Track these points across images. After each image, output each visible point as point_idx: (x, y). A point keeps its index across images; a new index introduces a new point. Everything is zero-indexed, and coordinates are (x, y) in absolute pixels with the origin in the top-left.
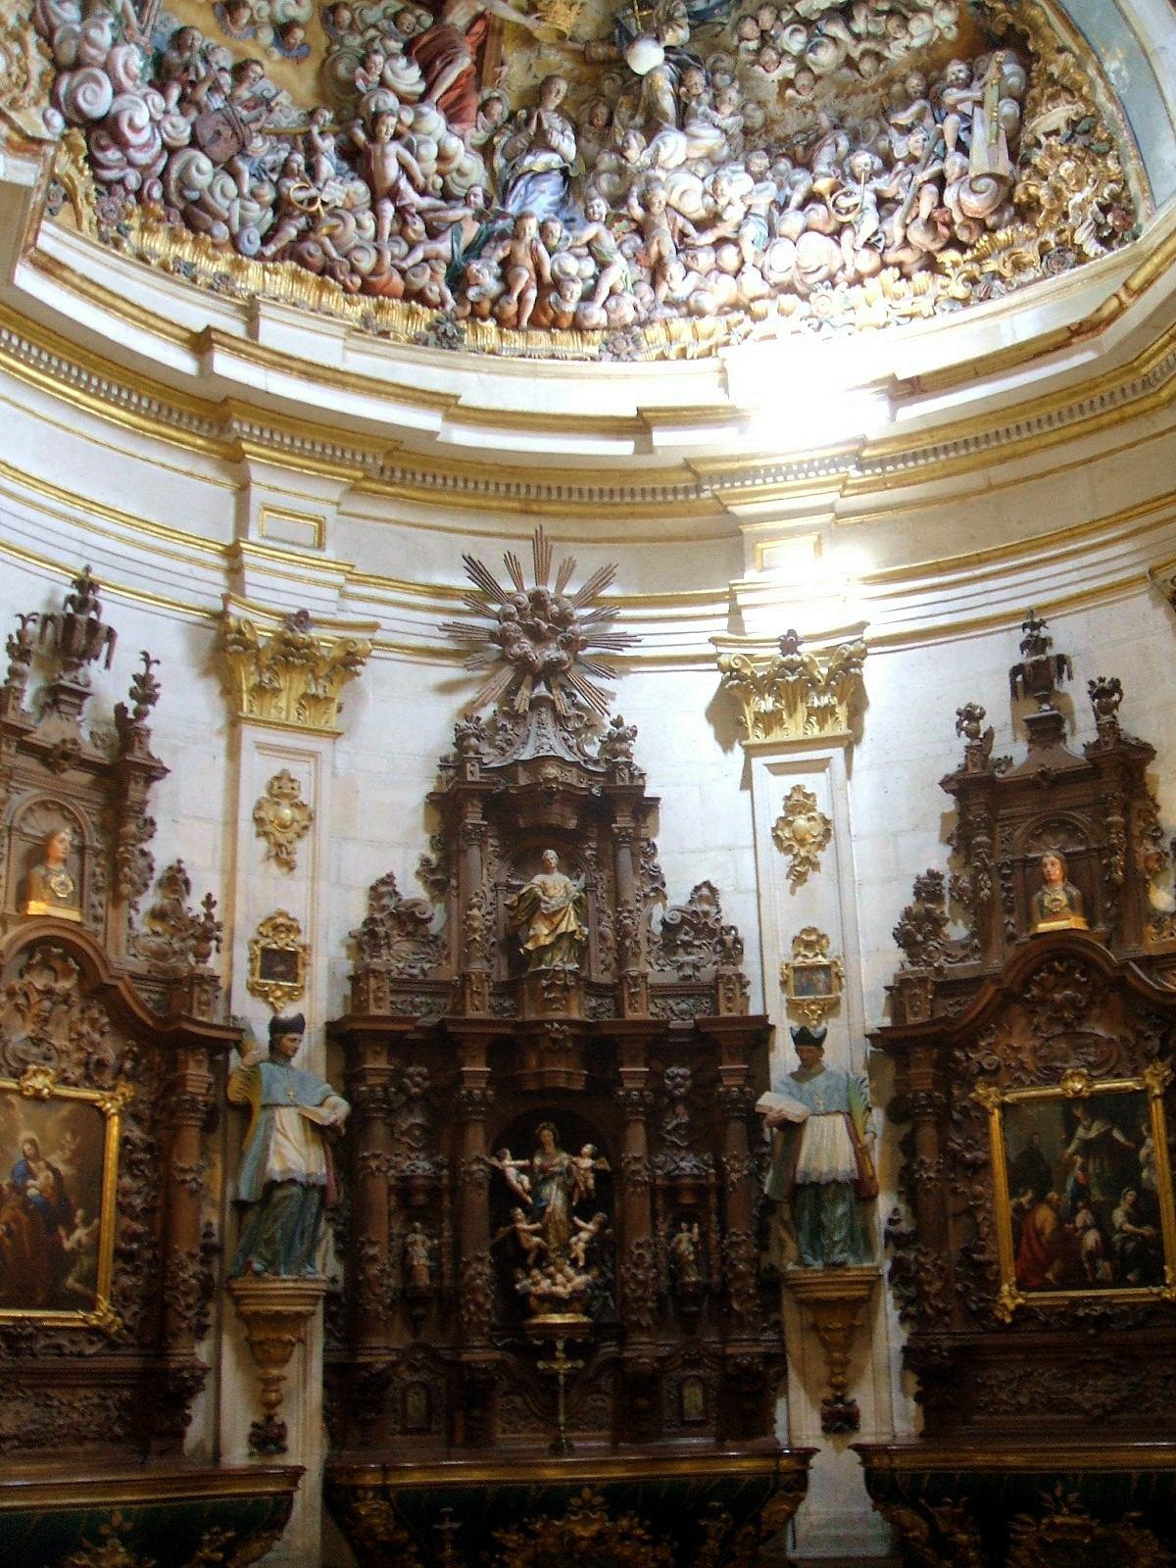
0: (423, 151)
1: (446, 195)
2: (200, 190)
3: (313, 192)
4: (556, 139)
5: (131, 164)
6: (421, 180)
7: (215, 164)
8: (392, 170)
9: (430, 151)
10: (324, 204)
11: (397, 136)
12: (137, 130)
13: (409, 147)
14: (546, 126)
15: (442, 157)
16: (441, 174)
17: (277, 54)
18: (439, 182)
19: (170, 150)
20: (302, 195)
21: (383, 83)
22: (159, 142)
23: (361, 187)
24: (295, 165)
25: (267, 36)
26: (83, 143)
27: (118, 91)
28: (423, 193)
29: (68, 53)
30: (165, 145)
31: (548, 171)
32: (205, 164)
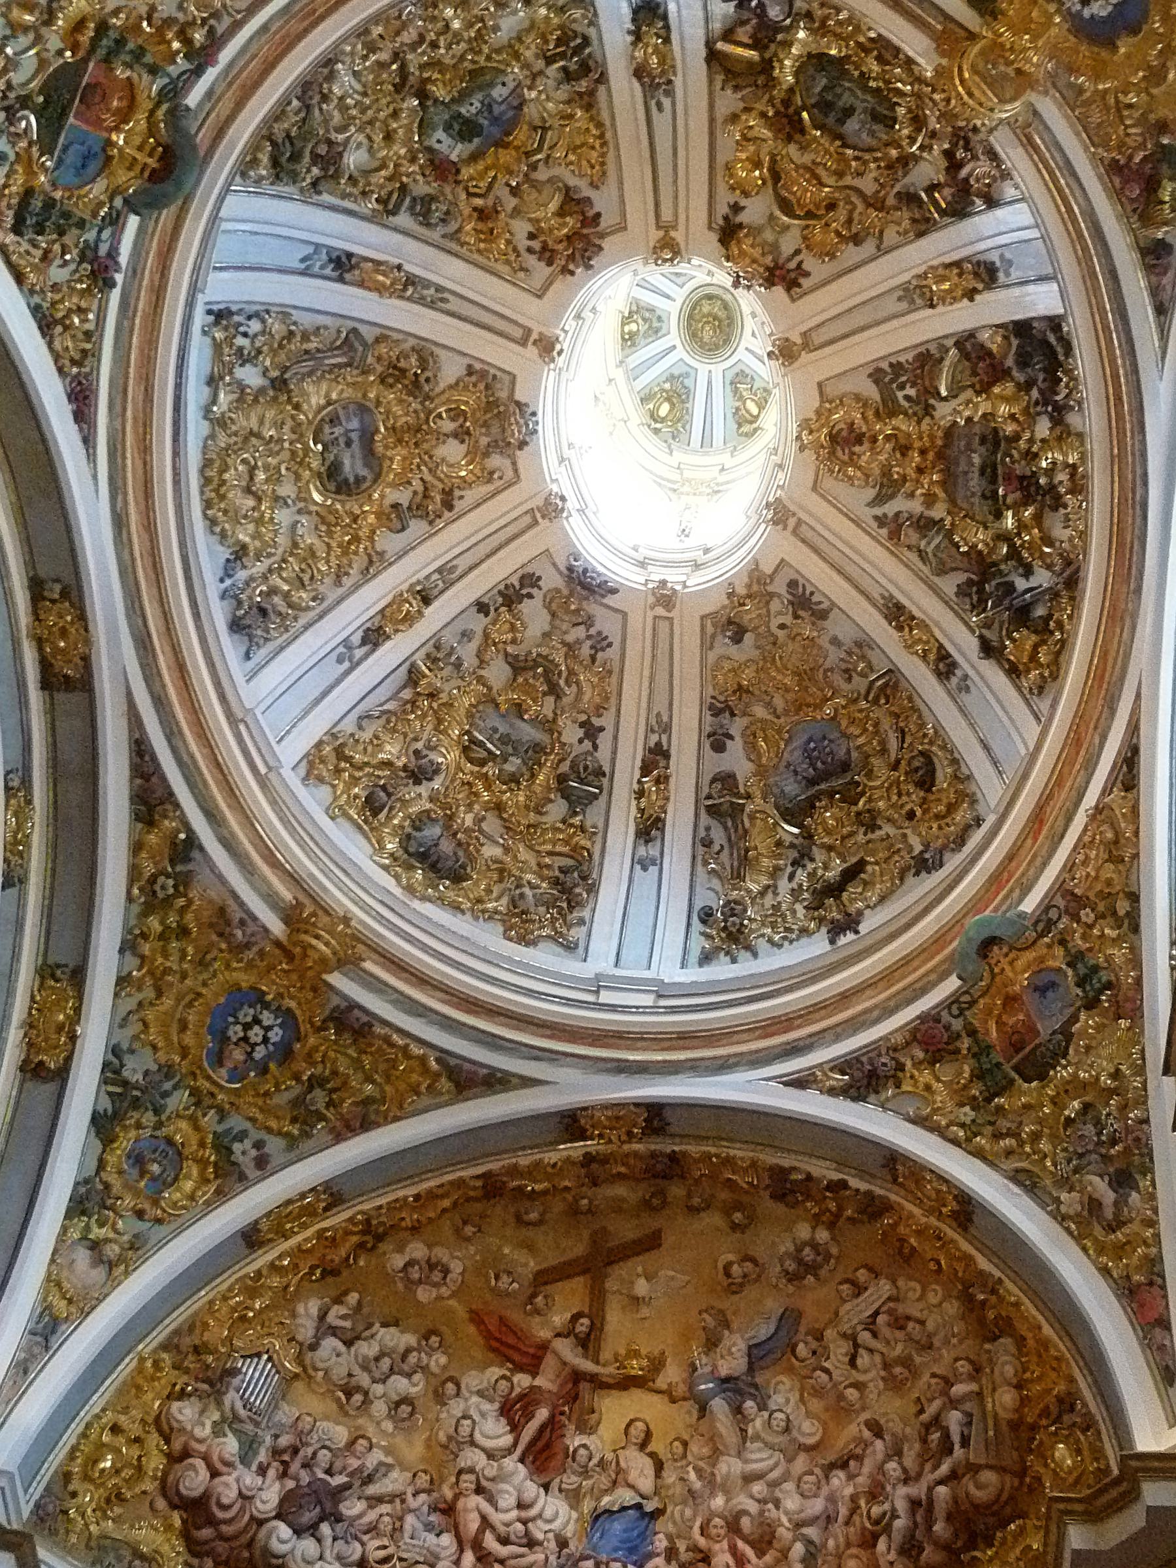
0: (502, 1504)
1: (531, 1543)
2: (284, 1556)
3: (390, 1550)
4: (633, 1477)
5: (221, 1537)
6: (502, 1529)
7: (298, 1532)
8: (472, 1524)
9: (507, 1500)
10: (401, 1559)
11: (479, 1490)
12: (225, 1508)
13: (492, 1500)
14: (623, 1464)
15: (521, 1506)
16: (525, 1522)
17: (388, 1426)
18: (519, 1526)
19: (261, 1523)
20: (381, 1554)
21: (473, 1443)
22: (247, 1518)
23: (447, 1540)
24: (382, 1526)
25: (379, 1408)
26: (178, 1523)
27: (215, 1474)
28: (504, 1541)
29: (177, 1445)
30: (252, 1518)
31: (624, 1509)
32: (284, 1530)
